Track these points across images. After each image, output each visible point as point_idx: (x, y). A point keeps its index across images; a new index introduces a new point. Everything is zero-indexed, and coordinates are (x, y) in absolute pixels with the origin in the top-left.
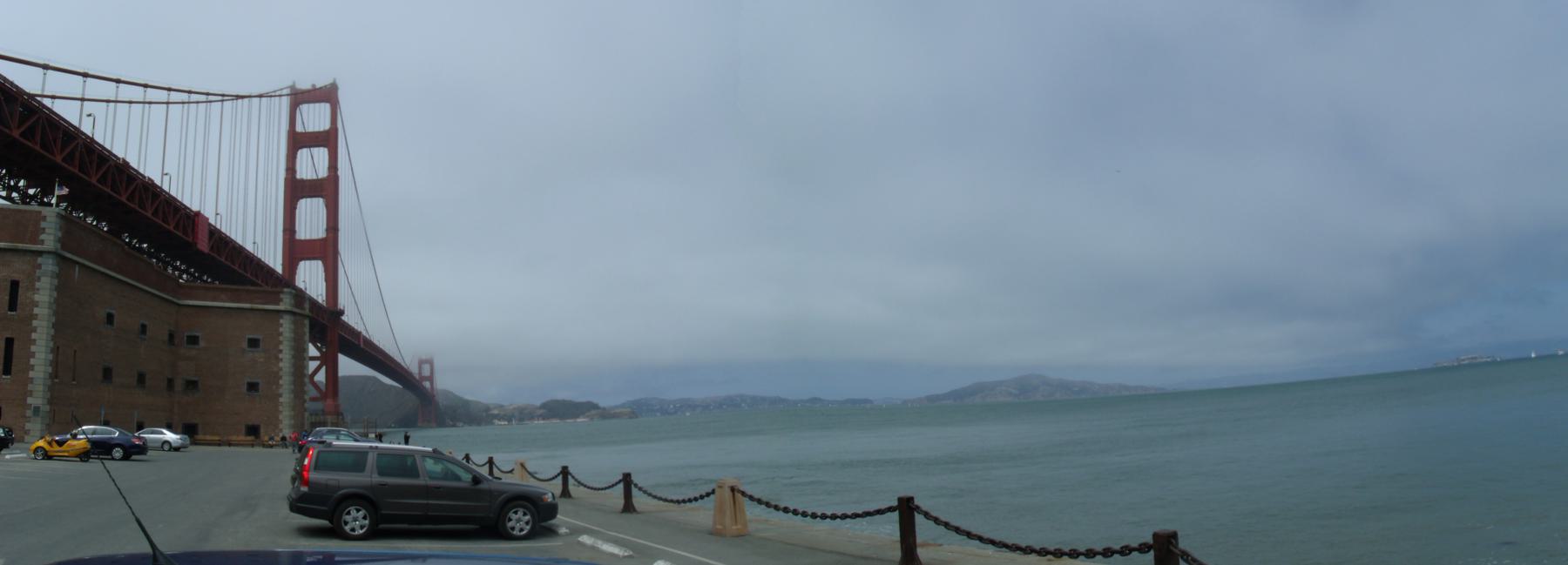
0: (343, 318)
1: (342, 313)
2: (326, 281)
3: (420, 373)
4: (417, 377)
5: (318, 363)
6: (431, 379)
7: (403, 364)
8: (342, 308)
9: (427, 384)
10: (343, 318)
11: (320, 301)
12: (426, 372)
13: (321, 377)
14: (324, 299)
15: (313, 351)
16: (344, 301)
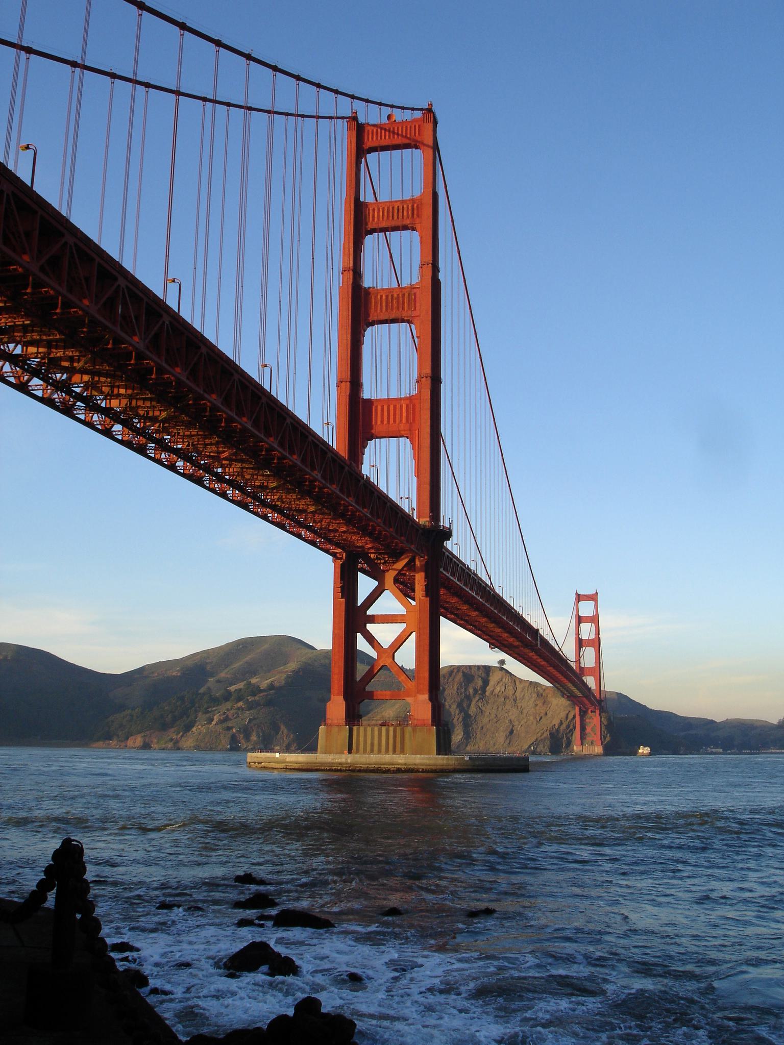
0: (448, 544)
1: (447, 534)
2: (418, 475)
3: (578, 661)
4: (573, 665)
5: (398, 628)
6: (597, 671)
7: (552, 642)
8: (447, 525)
9: (590, 681)
10: (448, 544)
11: (406, 507)
12: (588, 658)
13: (407, 657)
14: (415, 506)
15: (389, 603)
16: (449, 513)
